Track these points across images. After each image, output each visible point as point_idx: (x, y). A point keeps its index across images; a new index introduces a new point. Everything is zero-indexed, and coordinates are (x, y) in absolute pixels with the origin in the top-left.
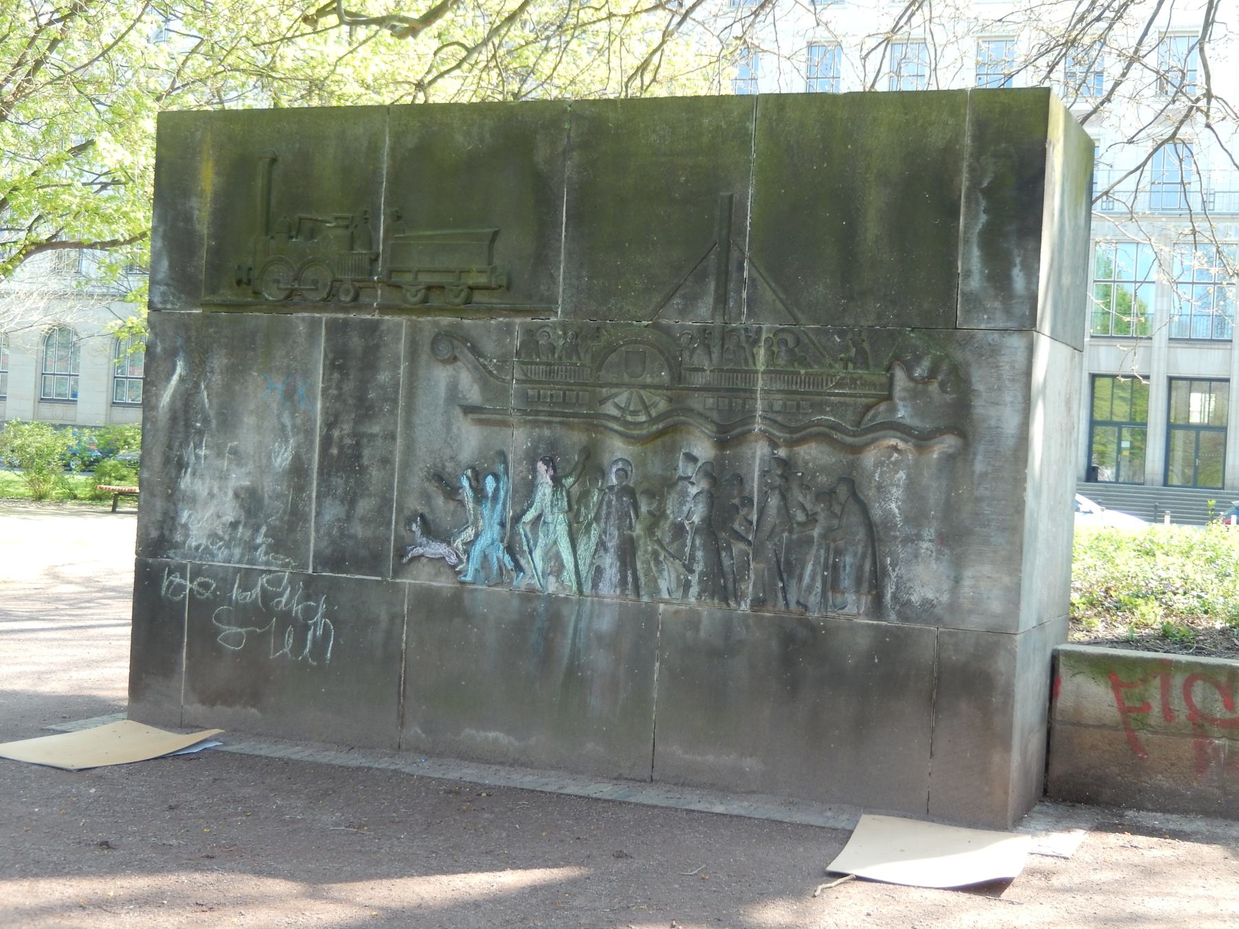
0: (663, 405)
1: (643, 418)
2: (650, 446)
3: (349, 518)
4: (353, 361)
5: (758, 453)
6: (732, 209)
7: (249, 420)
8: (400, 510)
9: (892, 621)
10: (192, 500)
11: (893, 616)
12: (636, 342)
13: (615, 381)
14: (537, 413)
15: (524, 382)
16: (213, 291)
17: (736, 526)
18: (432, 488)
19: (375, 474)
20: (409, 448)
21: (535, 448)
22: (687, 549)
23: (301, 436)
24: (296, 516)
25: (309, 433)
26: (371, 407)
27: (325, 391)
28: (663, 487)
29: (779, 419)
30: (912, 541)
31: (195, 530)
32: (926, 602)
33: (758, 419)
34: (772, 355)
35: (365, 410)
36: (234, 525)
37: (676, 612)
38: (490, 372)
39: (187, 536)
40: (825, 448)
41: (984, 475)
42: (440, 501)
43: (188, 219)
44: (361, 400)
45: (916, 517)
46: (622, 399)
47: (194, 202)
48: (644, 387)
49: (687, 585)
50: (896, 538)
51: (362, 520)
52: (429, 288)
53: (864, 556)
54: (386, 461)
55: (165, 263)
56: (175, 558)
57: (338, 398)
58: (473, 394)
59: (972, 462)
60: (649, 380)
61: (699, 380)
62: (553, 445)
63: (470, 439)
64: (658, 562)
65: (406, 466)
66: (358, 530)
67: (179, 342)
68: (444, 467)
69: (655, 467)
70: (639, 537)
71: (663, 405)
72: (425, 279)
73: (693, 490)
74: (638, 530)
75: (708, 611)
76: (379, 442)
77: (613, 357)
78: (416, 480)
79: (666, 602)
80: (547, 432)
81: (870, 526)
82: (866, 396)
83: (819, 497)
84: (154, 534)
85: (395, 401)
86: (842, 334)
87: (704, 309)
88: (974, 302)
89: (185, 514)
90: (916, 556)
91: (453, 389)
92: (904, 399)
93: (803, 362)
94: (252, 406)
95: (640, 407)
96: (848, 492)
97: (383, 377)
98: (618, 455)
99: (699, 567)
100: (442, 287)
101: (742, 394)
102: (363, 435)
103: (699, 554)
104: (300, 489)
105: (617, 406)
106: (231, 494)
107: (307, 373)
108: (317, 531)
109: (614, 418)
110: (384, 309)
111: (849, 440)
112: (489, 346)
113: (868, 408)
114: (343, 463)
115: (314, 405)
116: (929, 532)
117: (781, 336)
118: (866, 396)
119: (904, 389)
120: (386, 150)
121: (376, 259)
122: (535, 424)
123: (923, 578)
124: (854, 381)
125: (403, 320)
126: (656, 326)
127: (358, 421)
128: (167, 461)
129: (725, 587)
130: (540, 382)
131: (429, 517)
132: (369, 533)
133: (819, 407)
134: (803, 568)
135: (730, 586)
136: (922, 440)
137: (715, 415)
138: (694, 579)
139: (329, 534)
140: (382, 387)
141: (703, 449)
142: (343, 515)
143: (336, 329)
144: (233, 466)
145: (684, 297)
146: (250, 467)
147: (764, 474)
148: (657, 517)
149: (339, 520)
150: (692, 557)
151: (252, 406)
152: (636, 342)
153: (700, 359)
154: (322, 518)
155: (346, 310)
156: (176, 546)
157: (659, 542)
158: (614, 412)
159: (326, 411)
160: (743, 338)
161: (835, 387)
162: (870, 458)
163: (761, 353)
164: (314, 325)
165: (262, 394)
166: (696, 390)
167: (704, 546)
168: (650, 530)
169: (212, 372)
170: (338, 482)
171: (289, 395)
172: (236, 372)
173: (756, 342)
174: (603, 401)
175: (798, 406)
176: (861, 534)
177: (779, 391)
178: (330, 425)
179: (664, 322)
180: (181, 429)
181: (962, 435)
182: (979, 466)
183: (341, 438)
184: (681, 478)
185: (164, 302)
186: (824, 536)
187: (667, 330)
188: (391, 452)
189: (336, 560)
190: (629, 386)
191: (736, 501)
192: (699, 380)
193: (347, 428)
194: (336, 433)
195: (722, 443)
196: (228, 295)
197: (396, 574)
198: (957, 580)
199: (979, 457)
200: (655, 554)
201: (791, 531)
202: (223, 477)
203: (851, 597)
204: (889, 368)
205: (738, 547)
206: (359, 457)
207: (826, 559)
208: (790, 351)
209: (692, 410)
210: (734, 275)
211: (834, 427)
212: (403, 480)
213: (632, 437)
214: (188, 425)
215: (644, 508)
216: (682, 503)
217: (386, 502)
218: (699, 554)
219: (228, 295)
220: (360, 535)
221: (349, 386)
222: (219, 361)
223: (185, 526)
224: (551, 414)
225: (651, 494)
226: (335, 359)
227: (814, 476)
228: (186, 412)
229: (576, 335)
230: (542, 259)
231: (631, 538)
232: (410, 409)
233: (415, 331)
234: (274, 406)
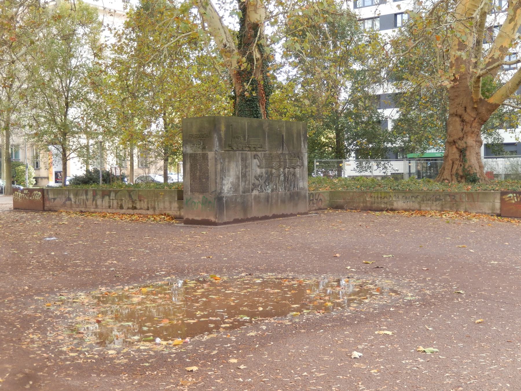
4: (244, 159)
5: (287, 170)
6: (283, 136)
7: (231, 170)
16: (225, 148)
19: (248, 177)
20: (252, 173)
24: (239, 185)
28: (279, 176)
35: (246, 167)
43: (221, 135)
45: (300, 177)
47: (221, 132)
54: (249, 175)
58: (259, 164)
62: (267, 171)
63: (259, 171)
66: (247, 186)
78: (253, 178)
91: (256, 163)
96: (294, 175)
97: (248, 162)
104: (239, 181)
107: (238, 161)
112: (260, 156)
114: (244, 176)
128: (220, 178)
136: (300, 167)
148: (279, 179)
164: (239, 153)
165: (233, 165)
171: (237, 165)
172: (229, 162)
178: (242, 170)
196: (227, 149)
202: (228, 180)
222: (227, 160)
230: (265, 143)
233: (251, 154)
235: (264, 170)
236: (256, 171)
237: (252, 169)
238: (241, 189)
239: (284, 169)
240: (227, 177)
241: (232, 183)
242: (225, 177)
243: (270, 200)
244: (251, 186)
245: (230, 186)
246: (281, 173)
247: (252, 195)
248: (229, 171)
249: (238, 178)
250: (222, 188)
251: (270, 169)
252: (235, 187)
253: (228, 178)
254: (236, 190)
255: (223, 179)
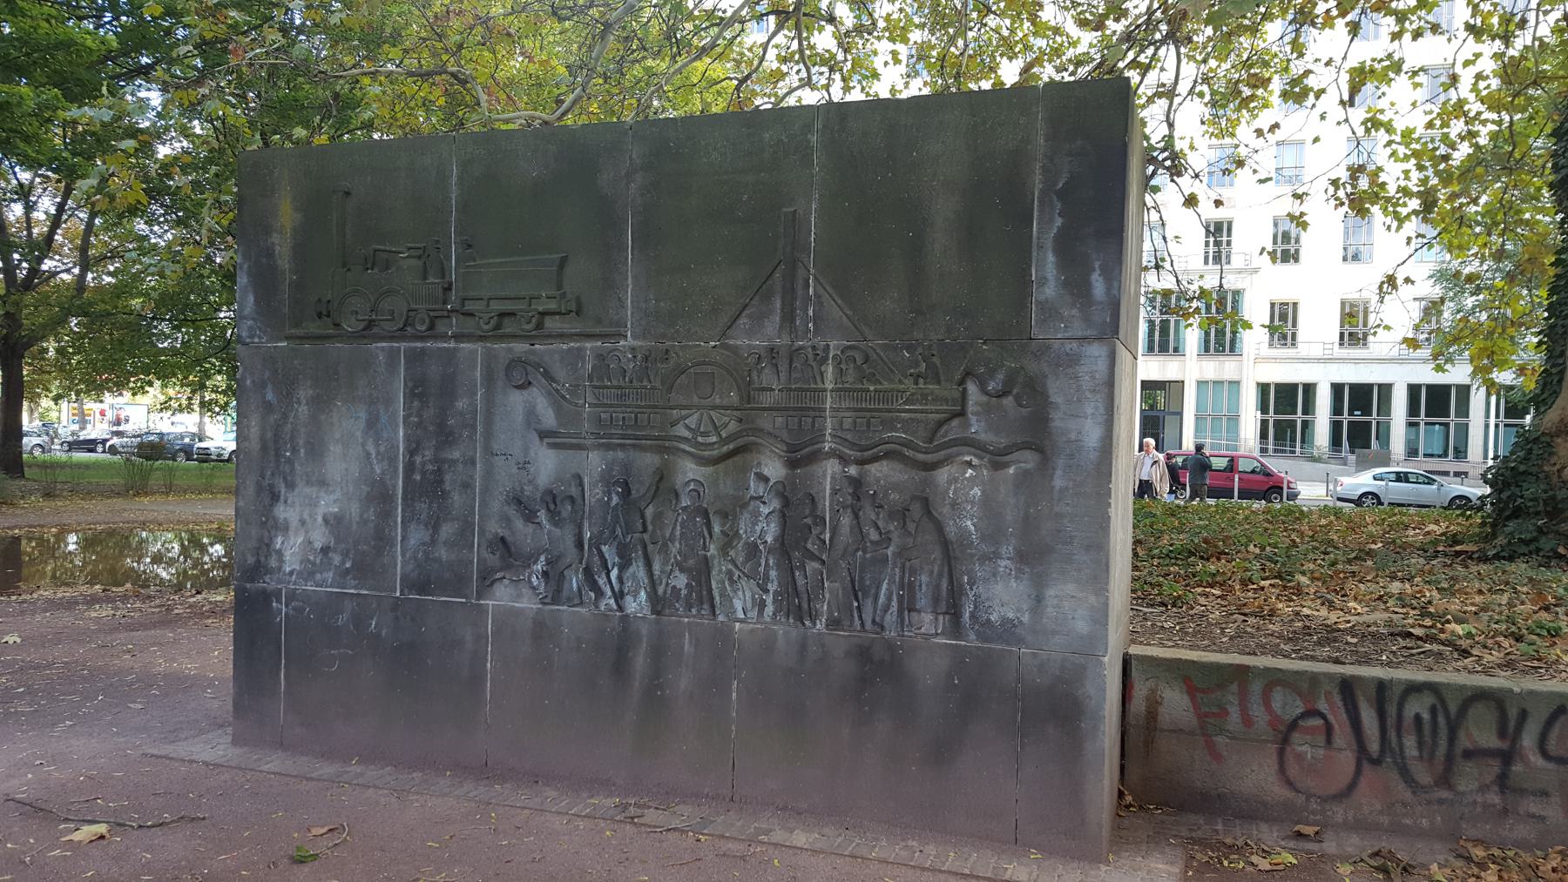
0: (733, 426)
1: (714, 439)
2: (721, 466)
3: (433, 542)
7: (335, 449)
8: (482, 532)
9: (971, 641)
10: (285, 528)
11: (972, 637)
12: (704, 363)
13: (684, 403)
14: (610, 436)
15: (596, 405)
16: (297, 325)
17: (809, 546)
18: (512, 511)
19: (457, 498)
20: (489, 473)
21: (609, 469)
22: (762, 569)
23: (386, 463)
24: (382, 540)
25: (393, 460)
26: (451, 433)
27: (406, 418)
29: (849, 437)
30: (990, 559)
31: (287, 556)
32: (1005, 621)
33: (828, 438)
34: (840, 373)
35: (446, 437)
36: (325, 550)
37: (752, 631)
38: (563, 397)
39: (281, 560)
40: (898, 466)
41: (1063, 490)
42: (519, 523)
43: (270, 254)
44: (441, 426)
45: (993, 536)
46: (692, 421)
47: (275, 238)
48: (714, 408)
49: (762, 605)
50: (972, 556)
51: (445, 543)
52: (502, 315)
53: (940, 575)
54: (467, 486)
55: (251, 298)
56: (269, 583)
57: (419, 424)
58: (549, 418)
59: (1052, 476)
60: (718, 401)
61: (767, 399)
62: (627, 467)
63: (547, 465)
64: (732, 582)
65: (485, 490)
66: (443, 553)
67: (267, 374)
68: (522, 490)
69: (726, 487)
70: (713, 557)
71: (733, 426)
72: (497, 306)
73: (765, 510)
74: (713, 550)
75: (785, 631)
76: (460, 467)
77: (683, 379)
78: (496, 506)
79: (741, 621)
80: (620, 454)
81: (945, 544)
82: (937, 412)
83: (891, 516)
84: (251, 560)
85: (474, 427)
86: (908, 348)
87: (772, 324)
88: (1050, 312)
89: (279, 540)
90: (994, 575)
92: (976, 414)
93: (872, 378)
94: (337, 435)
95: (711, 428)
96: (922, 509)
97: (461, 404)
98: (691, 476)
99: (772, 587)
100: (513, 314)
101: (812, 413)
102: (444, 461)
103: (773, 574)
104: (387, 514)
105: (687, 427)
106: (320, 519)
107: (389, 401)
108: (403, 555)
109: (686, 440)
110: (458, 337)
111: (921, 457)
113: (940, 424)
114: (428, 488)
115: (396, 432)
116: (1007, 550)
117: (850, 353)
118: (937, 412)
119: (977, 403)
120: (454, 179)
121: (449, 289)
122: (609, 447)
123: (1002, 595)
124: (924, 396)
125: (478, 347)
126: (725, 346)
127: (438, 448)
128: (259, 488)
129: (800, 606)
130: (611, 406)
131: (509, 539)
132: (453, 557)
133: (889, 425)
134: (878, 588)
135: (805, 606)
137: (785, 436)
138: (769, 599)
139: (416, 559)
140: (461, 414)
141: (774, 469)
142: (427, 539)
143: (414, 358)
144: (322, 494)
145: (749, 317)
146: (338, 495)
147: (835, 492)
148: (730, 539)
149: (424, 544)
150: (767, 578)
151: (337, 435)
152: (704, 363)
153: (767, 377)
154: (407, 545)
155: (422, 338)
156: (269, 571)
157: (733, 562)
158: (687, 434)
159: (407, 438)
160: (810, 356)
161: (905, 403)
162: (942, 475)
163: (830, 370)
164: (393, 355)
166: (764, 409)
167: (778, 566)
168: (724, 550)
169: (299, 403)
170: (422, 506)
171: (372, 424)
172: (321, 403)
173: (824, 360)
174: (673, 424)
175: (868, 425)
176: (937, 554)
177: (848, 409)
178: (412, 452)
179: (731, 342)
180: (272, 459)
181: (1040, 450)
182: (1058, 483)
183: (423, 464)
184: (752, 498)
185: (252, 337)
186: (898, 555)
187: (735, 350)
188: (472, 477)
189: (421, 584)
190: (698, 408)
191: (809, 521)
192: (767, 399)
193: (429, 454)
194: (418, 459)
195: (792, 464)
196: (313, 328)
197: (480, 596)
198: (1039, 599)
199: (1059, 472)
200: (730, 573)
201: (865, 552)
202: (313, 504)
203: (927, 617)
204: (962, 382)
205: (812, 566)
206: (441, 482)
207: (902, 578)
208: (858, 368)
209: (762, 430)
210: (800, 292)
211: (906, 444)
212: (484, 504)
213: (702, 458)
214: (278, 455)
215: (717, 529)
216: (755, 524)
217: (467, 527)
218: (773, 574)
219: (313, 328)
220: (444, 558)
221: (429, 413)
222: (304, 393)
223: (280, 553)
224: (623, 437)
225: (724, 516)
226: (416, 387)
227: (886, 495)
228: (276, 442)
229: (646, 359)
231: (706, 557)
232: (488, 435)
233: (490, 358)
234: (359, 434)
235: (593, 463)
236: (524, 466)
237: (489, 452)
238: (400, 563)
239: (800, 457)
240: (303, 490)
241: (334, 523)
242: (291, 486)
243: (640, 661)
244: (477, 554)
245: (320, 538)
246: (755, 488)
247: (482, 610)
248: (316, 452)
249: (380, 496)
250: (265, 547)
251: (648, 461)
252: (361, 552)
253: (311, 491)
254: (366, 567)
255: (275, 497)
